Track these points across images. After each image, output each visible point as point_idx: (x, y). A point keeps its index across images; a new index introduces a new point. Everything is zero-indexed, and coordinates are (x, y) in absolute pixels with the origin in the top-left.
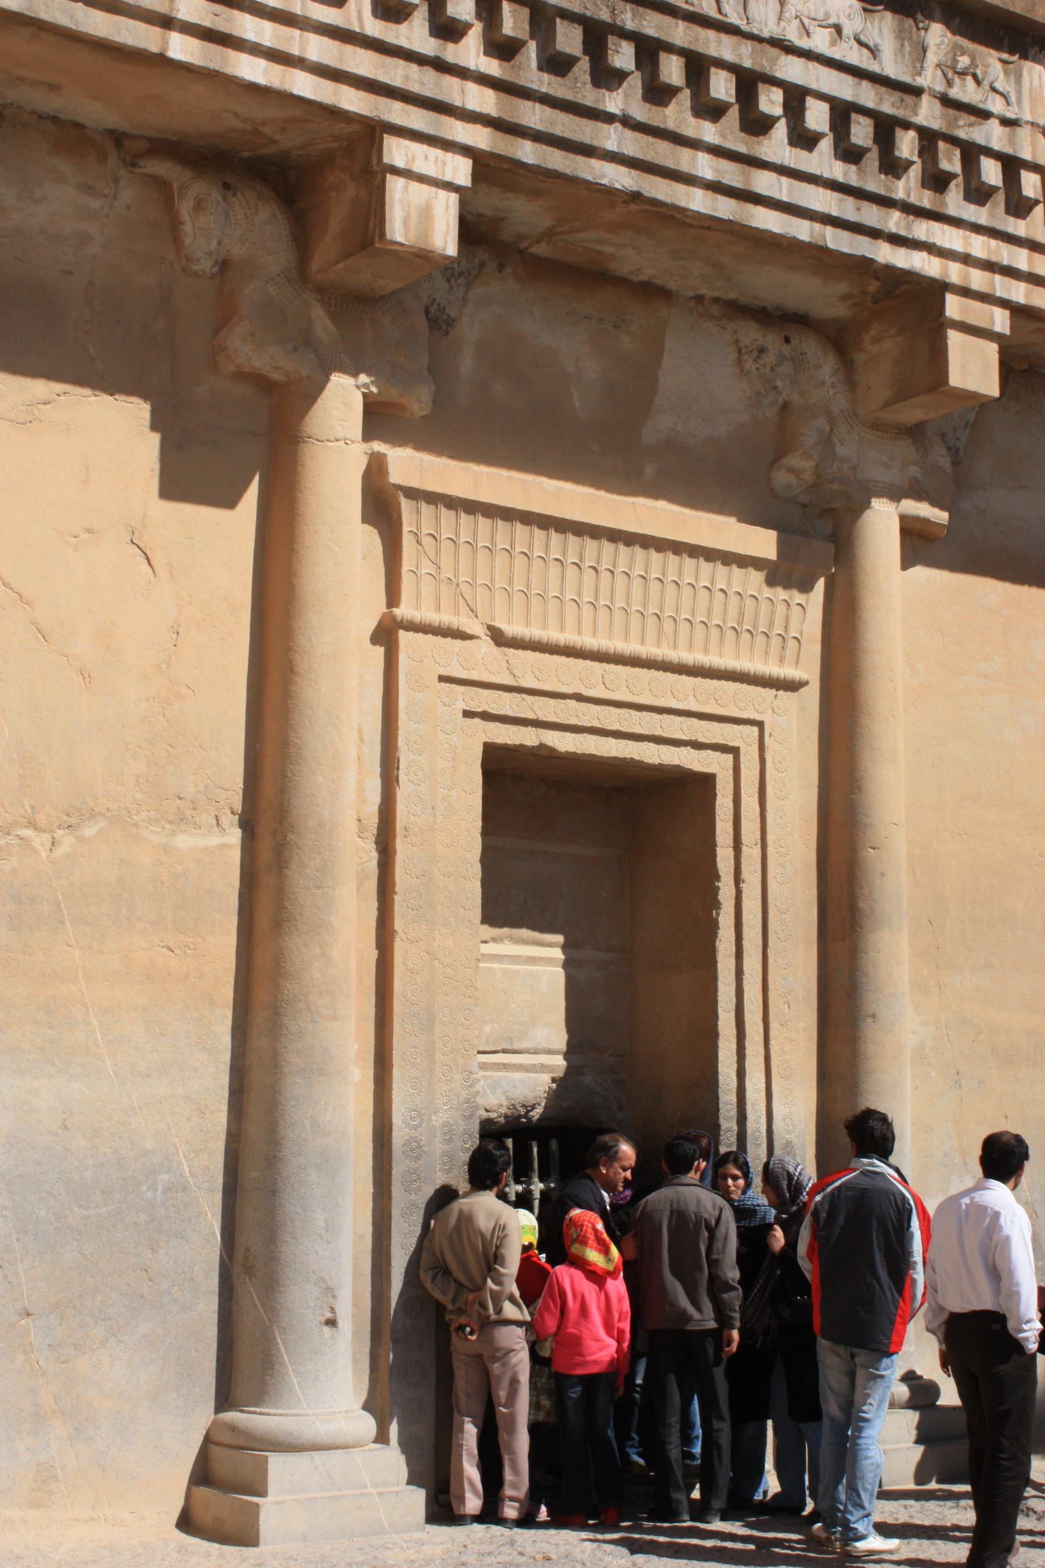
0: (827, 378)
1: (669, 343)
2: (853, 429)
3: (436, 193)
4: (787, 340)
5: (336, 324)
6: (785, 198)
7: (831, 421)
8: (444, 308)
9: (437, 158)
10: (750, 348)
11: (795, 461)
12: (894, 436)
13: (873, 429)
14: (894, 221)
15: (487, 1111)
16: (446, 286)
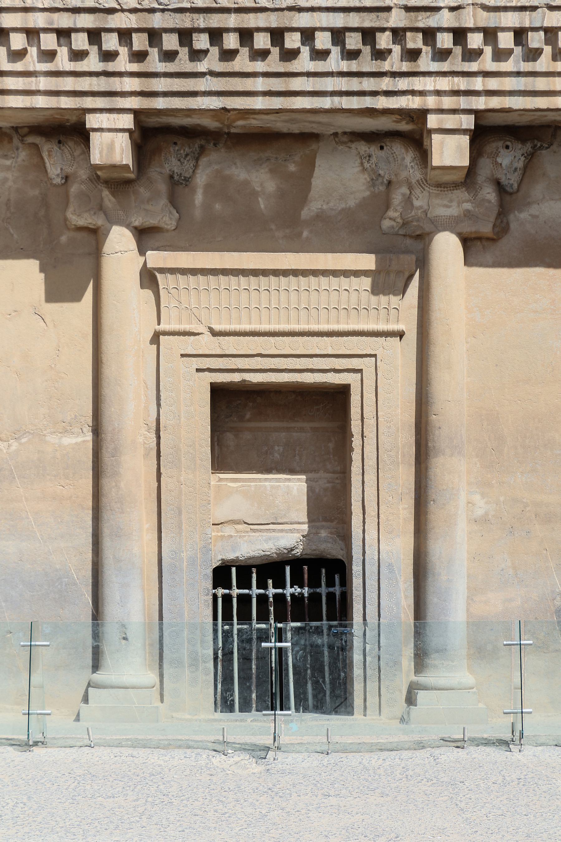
0: (408, 164)
1: (318, 162)
2: (424, 190)
3: (117, 135)
4: (382, 148)
5: (114, 197)
6: (310, 89)
7: (411, 188)
8: (181, 174)
9: (114, 118)
10: (365, 156)
11: (391, 213)
12: (452, 188)
13: (438, 187)
14: (386, 84)
15: (263, 551)
16: (179, 163)
